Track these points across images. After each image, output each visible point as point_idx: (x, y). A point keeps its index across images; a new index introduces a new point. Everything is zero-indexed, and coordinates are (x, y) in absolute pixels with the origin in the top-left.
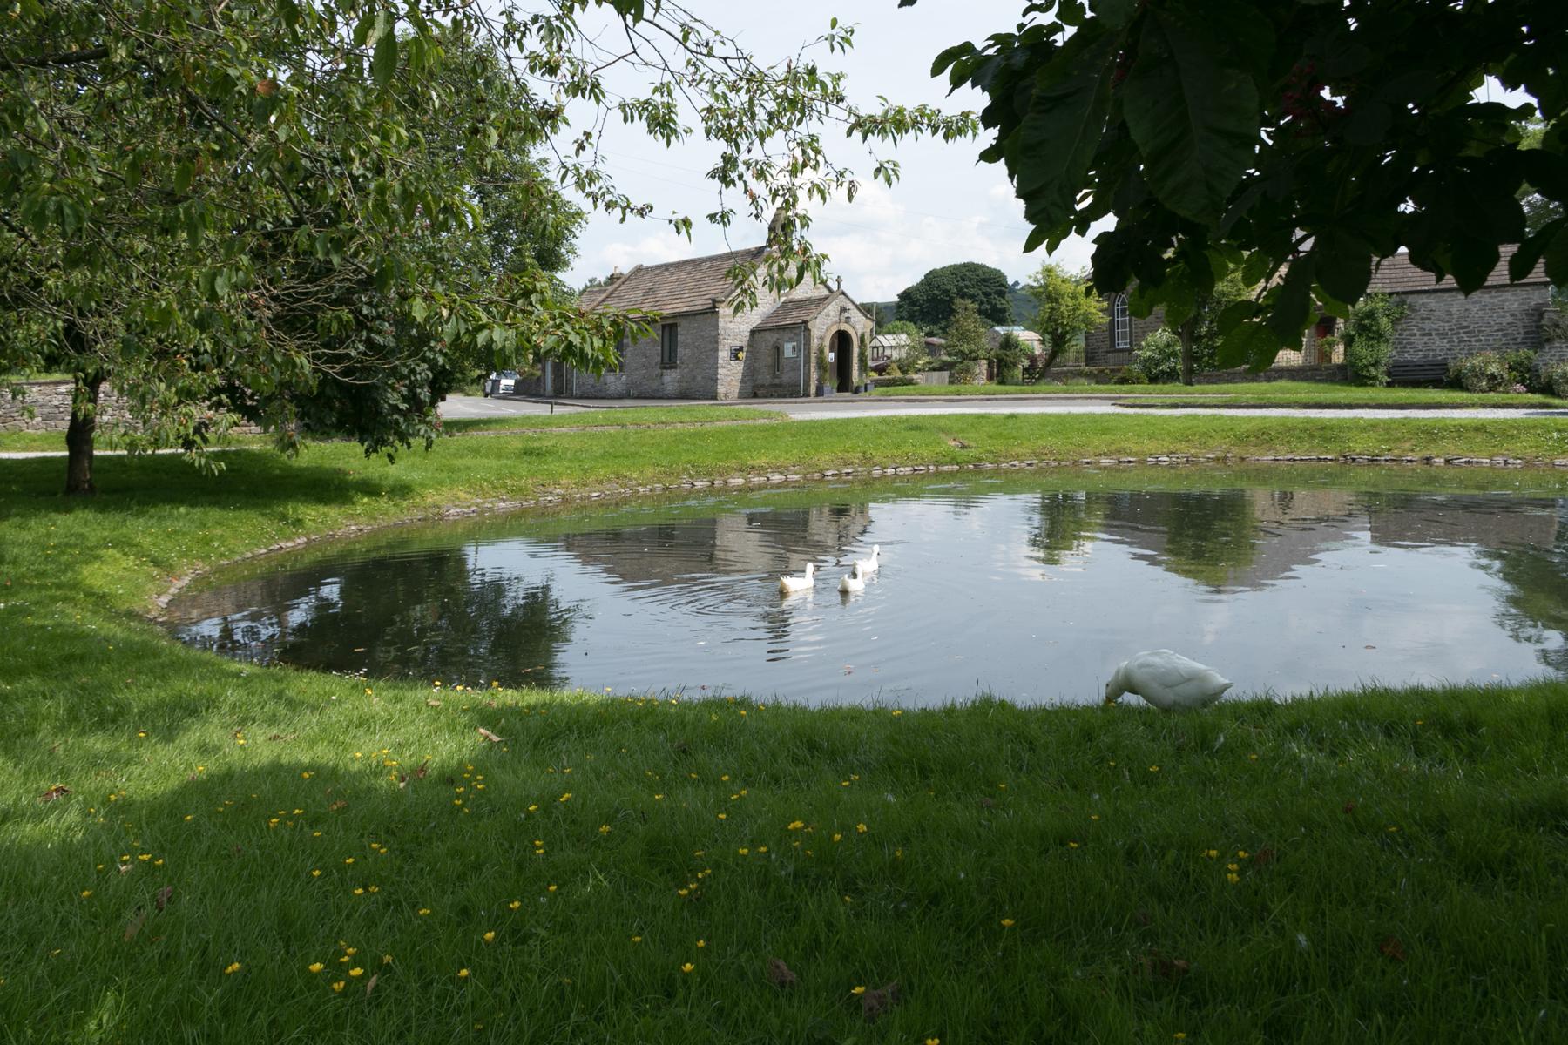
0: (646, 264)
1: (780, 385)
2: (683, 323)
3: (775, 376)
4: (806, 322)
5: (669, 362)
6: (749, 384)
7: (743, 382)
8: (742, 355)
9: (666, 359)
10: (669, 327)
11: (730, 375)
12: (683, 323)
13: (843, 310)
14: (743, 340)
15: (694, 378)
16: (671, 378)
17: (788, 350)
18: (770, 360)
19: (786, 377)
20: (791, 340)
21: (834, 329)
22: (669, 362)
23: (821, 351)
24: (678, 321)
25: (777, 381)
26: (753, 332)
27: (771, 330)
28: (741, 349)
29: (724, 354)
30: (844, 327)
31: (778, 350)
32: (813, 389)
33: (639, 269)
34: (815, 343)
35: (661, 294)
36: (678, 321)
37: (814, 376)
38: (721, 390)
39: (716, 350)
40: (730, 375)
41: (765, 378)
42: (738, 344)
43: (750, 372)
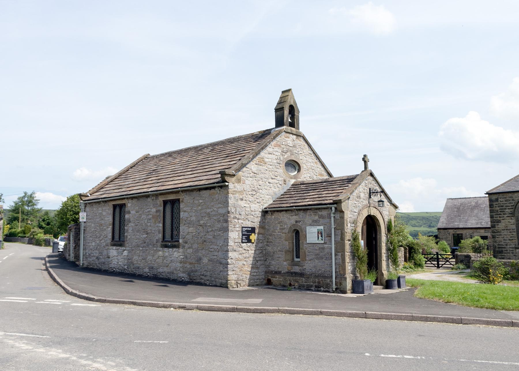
0: (152, 154)
1: (301, 275)
2: (185, 198)
3: (293, 264)
4: (338, 203)
5: (170, 240)
6: (262, 269)
7: (254, 266)
8: (253, 237)
9: (168, 237)
10: (171, 203)
11: (241, 260)
12: (185, 198)
13: (371, 193)
14: (255, 221)
15: (200, 260)
17: (312, 234)
19: (309, 265)
20: (315, 223)
21: (365, 214)
22: (170, 240)
23: (355, 239)
24: (181, 196)
25: (297, 269)
26: (265, 213)
27: (286, 211)
28: (253, 230)
29: (234, 235)
30: (374, 212)
31: (297, 235)
32: (349, 285)
33: (146, 158)
34: (349, 228)
35: (163, 174)
36: (181, 196)
37: (349, 267)
38: (232, 277)
39: (226, 230)
40: (241, 260)
41: (282, 263)
42: (249, 224)
43: (262, 257)
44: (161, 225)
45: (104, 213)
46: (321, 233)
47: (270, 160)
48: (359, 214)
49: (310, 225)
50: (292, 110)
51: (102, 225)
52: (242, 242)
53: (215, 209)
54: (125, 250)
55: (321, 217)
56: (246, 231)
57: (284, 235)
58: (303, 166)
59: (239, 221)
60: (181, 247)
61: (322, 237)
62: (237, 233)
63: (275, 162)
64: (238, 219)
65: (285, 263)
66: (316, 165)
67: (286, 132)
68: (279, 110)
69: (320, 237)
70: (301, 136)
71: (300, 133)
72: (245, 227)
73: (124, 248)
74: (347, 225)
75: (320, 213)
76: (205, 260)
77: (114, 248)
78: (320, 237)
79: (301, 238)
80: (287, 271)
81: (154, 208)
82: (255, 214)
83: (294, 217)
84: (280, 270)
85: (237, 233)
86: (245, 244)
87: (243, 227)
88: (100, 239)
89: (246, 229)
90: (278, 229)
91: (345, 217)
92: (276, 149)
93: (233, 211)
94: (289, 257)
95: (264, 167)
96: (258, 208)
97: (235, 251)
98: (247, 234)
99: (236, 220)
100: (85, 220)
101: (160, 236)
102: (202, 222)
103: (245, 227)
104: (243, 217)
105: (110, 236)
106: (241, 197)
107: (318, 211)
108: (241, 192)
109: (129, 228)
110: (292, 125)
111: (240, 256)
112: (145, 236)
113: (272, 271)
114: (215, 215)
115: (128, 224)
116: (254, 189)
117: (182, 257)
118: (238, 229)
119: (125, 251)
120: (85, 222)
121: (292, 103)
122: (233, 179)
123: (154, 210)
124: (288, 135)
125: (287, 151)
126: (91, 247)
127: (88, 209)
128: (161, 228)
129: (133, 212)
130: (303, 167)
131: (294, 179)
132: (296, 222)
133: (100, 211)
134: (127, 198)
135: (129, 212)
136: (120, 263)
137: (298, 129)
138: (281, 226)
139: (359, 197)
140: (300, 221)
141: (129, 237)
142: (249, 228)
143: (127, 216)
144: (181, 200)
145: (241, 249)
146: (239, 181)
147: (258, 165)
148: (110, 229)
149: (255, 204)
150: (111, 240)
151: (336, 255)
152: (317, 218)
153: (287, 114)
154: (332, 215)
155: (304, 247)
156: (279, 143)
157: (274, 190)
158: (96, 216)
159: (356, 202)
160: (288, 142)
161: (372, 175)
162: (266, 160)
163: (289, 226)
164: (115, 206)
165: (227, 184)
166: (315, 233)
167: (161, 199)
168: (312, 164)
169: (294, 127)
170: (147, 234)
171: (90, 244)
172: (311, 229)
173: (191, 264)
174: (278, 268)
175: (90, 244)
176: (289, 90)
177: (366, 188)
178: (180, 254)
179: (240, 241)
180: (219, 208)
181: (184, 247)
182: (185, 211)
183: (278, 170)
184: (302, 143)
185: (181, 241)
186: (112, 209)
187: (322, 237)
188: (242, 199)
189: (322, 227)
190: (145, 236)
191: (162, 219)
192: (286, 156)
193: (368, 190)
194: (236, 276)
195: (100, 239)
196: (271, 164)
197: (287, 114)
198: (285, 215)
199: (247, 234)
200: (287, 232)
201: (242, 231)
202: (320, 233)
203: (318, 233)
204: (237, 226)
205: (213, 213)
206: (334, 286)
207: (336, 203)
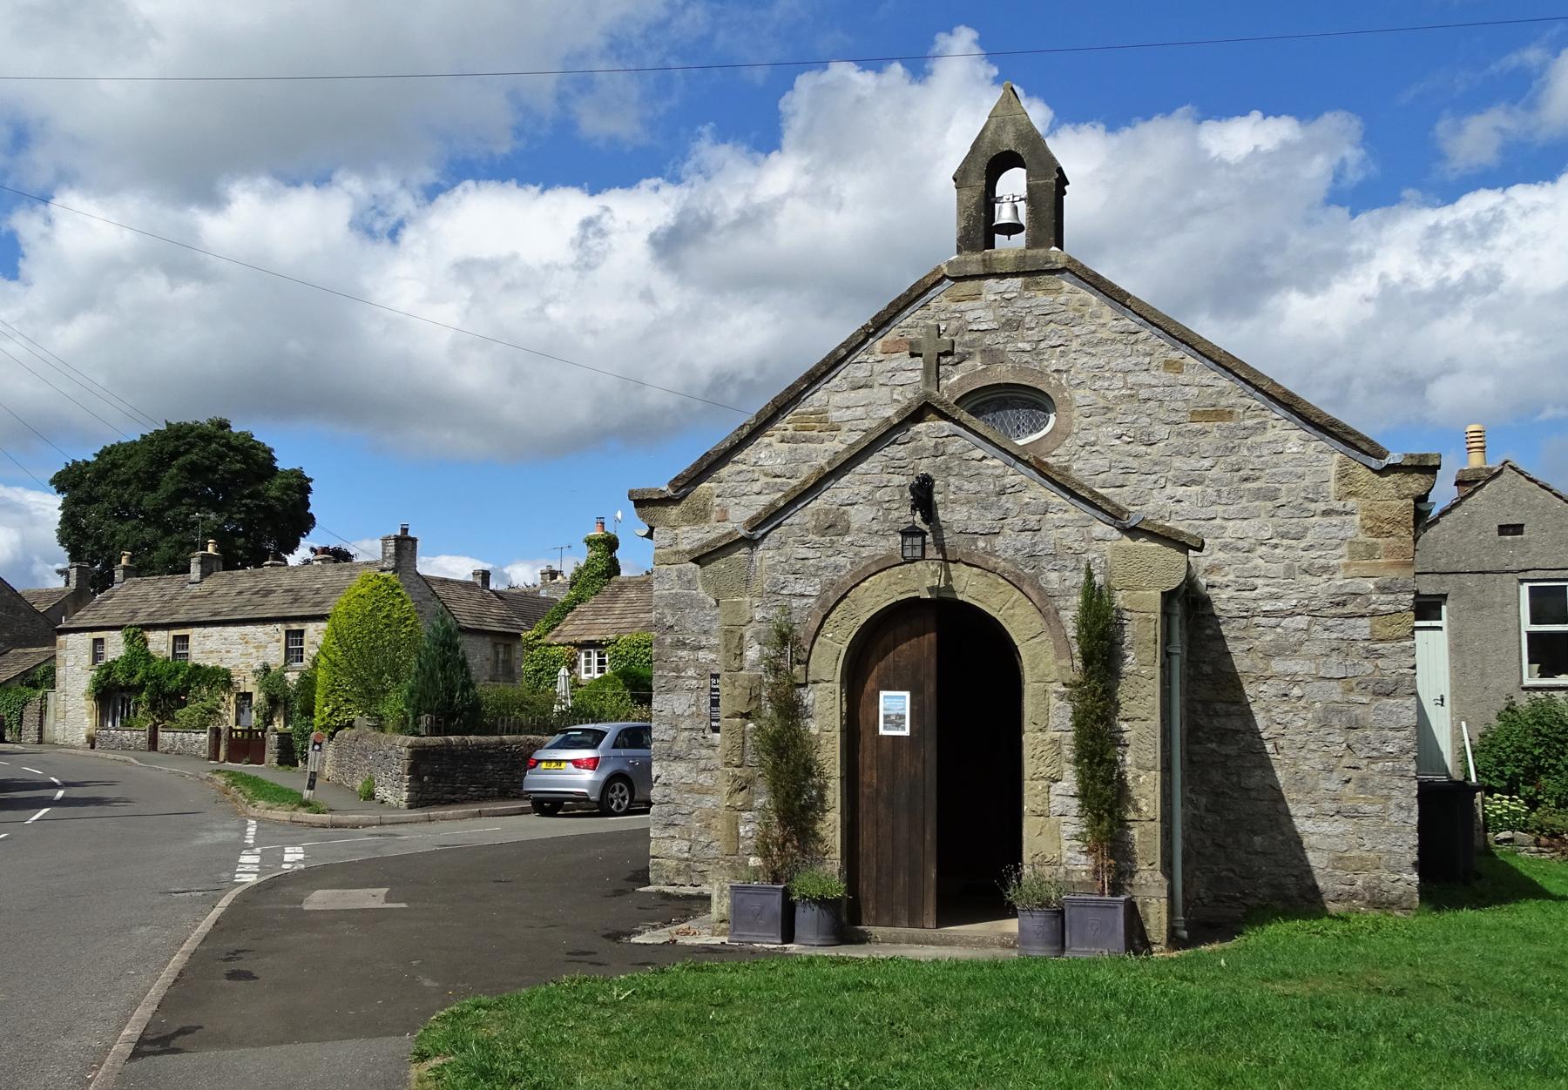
47: (860, 412)
59: (701, 654)
66: (1167, 377)
67: (956, 279)
93: (670, 621)
95: (827, 445)
97: (678, 758)
104: (714, 641)
111: (701, 778)
122: (673, 512)
124: (968, 287)
130: (1069, 402)
139: (833, 526)
147: (793, 440)
160: (970, 316)
162: (835, 416)
168: (1144, 378)
192: (955, 378)
194: (685, 845)
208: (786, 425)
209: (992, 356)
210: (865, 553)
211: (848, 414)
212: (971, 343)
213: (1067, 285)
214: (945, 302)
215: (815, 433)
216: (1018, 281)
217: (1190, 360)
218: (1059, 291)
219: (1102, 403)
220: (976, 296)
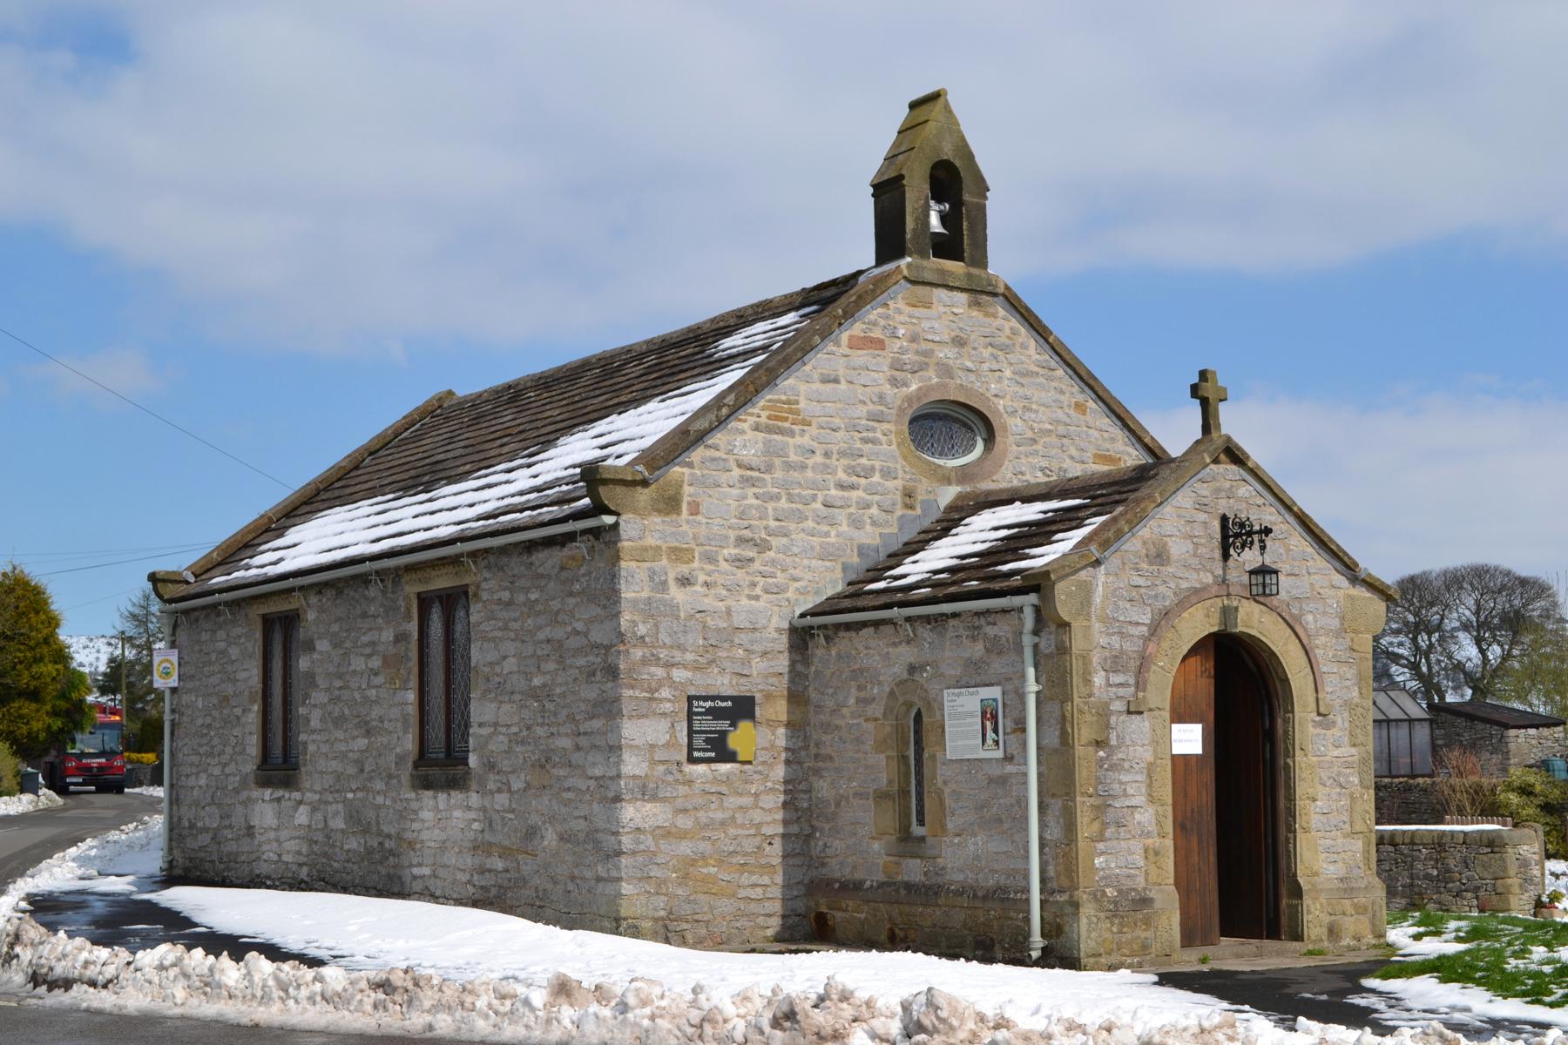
1: (929, 892)
2: (489, 586)
8: (741, 737)
12: (489, 586)
13: (1234, 534)
14: (764, 670)
16: (442, 821)
18: (881, 769)
19: (962, 854)
20: (973, 676)
25: (913, 870)
26: (801, 637)
28: (742, 708)
29: (649, 735)
30: (1254, 621)
41: (862, 848)
42: (724, 684)
44: (412, 696)
45: (234, 652)
46: (994, 717)
48: (1154, 629)
49: (958, 685)
50: (954, 181)
51: (226, 698)
52: (692, 760)
53: (579, 626)
54: (301, 802)
55: (995, 647)
56: (709, 711)
57: (870, 726)
58: (1012, 426)
60: (474, 785)
61: (996, 731)
62: (664, 724)
63: (862, 411)
64: (670, 665)
65: (876, 846)
68: (888, 192)
69: (990, 735)
70: (995, 295)
71: (990, 280)
72: (705, 698)
73: (296, 795)
74: (1088, 682)
75: (990, 631)
76: (550, 838)
77: (268, 793)
78: (990, 735)
79: (929, 739)
80: (881, 877)
81: (389, 629)
82: (752, 642)
83: (903, 649)
84: (858, 876)
85: (664, 724)
86: (701, 768)
87: (690, 699)
88: (225, 758)
89: (709, 704)
90: (852, 701)
91: (1077, 644)
92: (862, 357)
93: (642, 629)
94: (890, 821)
95: (798, 440)
96: (773, 616)
97: (654, 798)
98: (715, 725)
99: (660, 672)
100: (173, 681)
101: (409, 743)
102: (537, 681)
103: (705, 698)
104: (689, 657)
105: (253, 748)
106: (684, 569)
107: (983, 621)
108: (678, 554)
109: (312, 713)
110: (947, 247)
112: (362, 742)
113: (829, 883)
114: (578, 651)
115: (307, 696)
116: (747, 533)
117: (476, 826)
118: (668, 707)
119: (302, 809)
120: (174, 690)
121: (947, 152)
122: (643, 495)
123: (388, 635)
124: (920, 290)
125: (923, 367)
126: (195, 793)
127: (182, 637)
128: (412, 711)
129: (323, 645)
130: (1005, 429)
131: (960, 482)
132: (912, 669)
133: (222, 645)
134: (302, 588)
135: (310, 646)
136: (286, 858)
137: (981, 261)
138: (860, 688)
139: (1160, 556)
140: (922, 668)
141: (311, 748)
142: (724, 699)
143: (303, 663)
144: (471, 591)
145: (682, 790)
146: (670, 504)
147: (769, 430)
148: (253, 716)
149: (757, 598)
150: (257, 761)
151: (1042, 808)
152: (977, 650)
153: (930, 203)
154: (1028, 640)
155: (941, 776)
156: (877, 333)
157: (856, 534)
158: (210, 663)
159: (1141, 582)
161: (1235, 455)
163: (888, 689)
164: (268, 622)
165: (608, 520)
166: (971, 714)
167: (412, 588)
169: (957, 256)
170: (368, 733)
171: (192, 781)
172: (960, 701)
173: (505, 853)
174: (854, 867)
175: (192, 781)
176: (935, 97)
177: (1202, 517)
178: (472, 815)
179: (683, 756)
180: (591, 621)
181: (482, 783)
182: (485, 639)
183: (867, 448)
184: (999, 322)
185: (473, 760)
186: (258, 635)
187: (996, 731)
188: (685, 582)
189: (995, 692)
190: (362, 742)
191: (416, 670)
192: (914, 387)
193: (1216, 525)
195: (225, 758)
196: (837, 422)
197: (930, 203)
198: (872, 643)
199: (715, 725)
200: (879, 714)
201: (690, 714)
202: (989, 715)
203: (984, 714)
204: (665, 693)
205: (574, 642)
206: (1037, 941)
207: (1036, 589)
208: (759, 411)
209: (946, 370)
210: (1184, 585)
211: (816, 408)
212: (928, 354)
213: (1002, 312)
214: (901, 305)
215: (787, 425)
216: (963, 297)
217: (1091, 404)
218: (995, 316)
219: (1030, 434)
220: (928, 305)
